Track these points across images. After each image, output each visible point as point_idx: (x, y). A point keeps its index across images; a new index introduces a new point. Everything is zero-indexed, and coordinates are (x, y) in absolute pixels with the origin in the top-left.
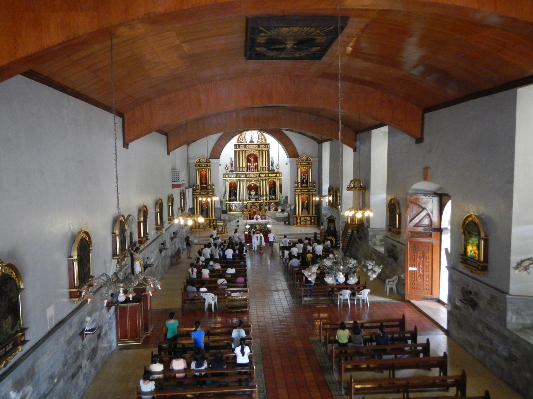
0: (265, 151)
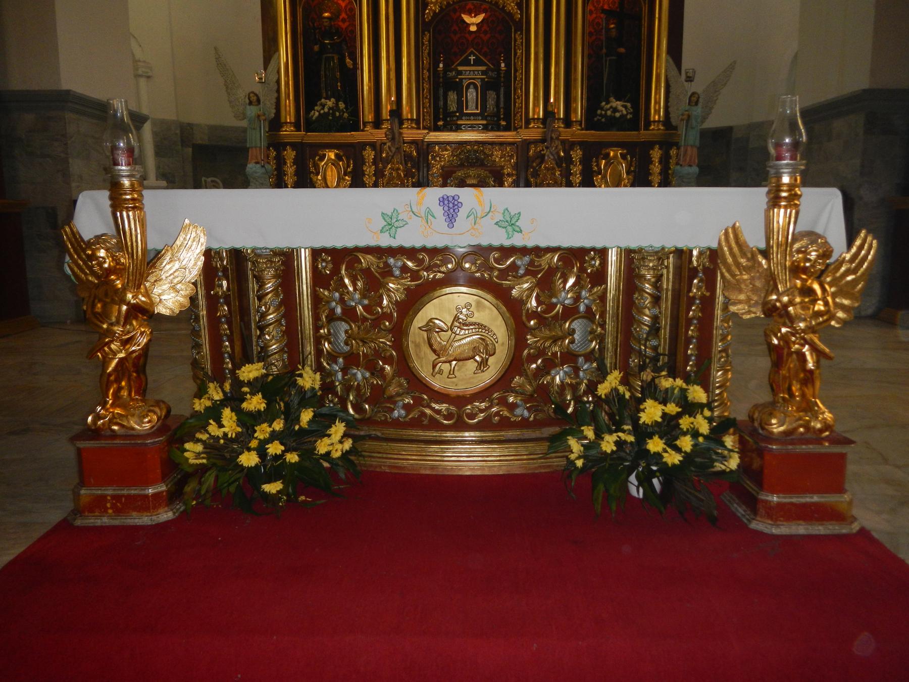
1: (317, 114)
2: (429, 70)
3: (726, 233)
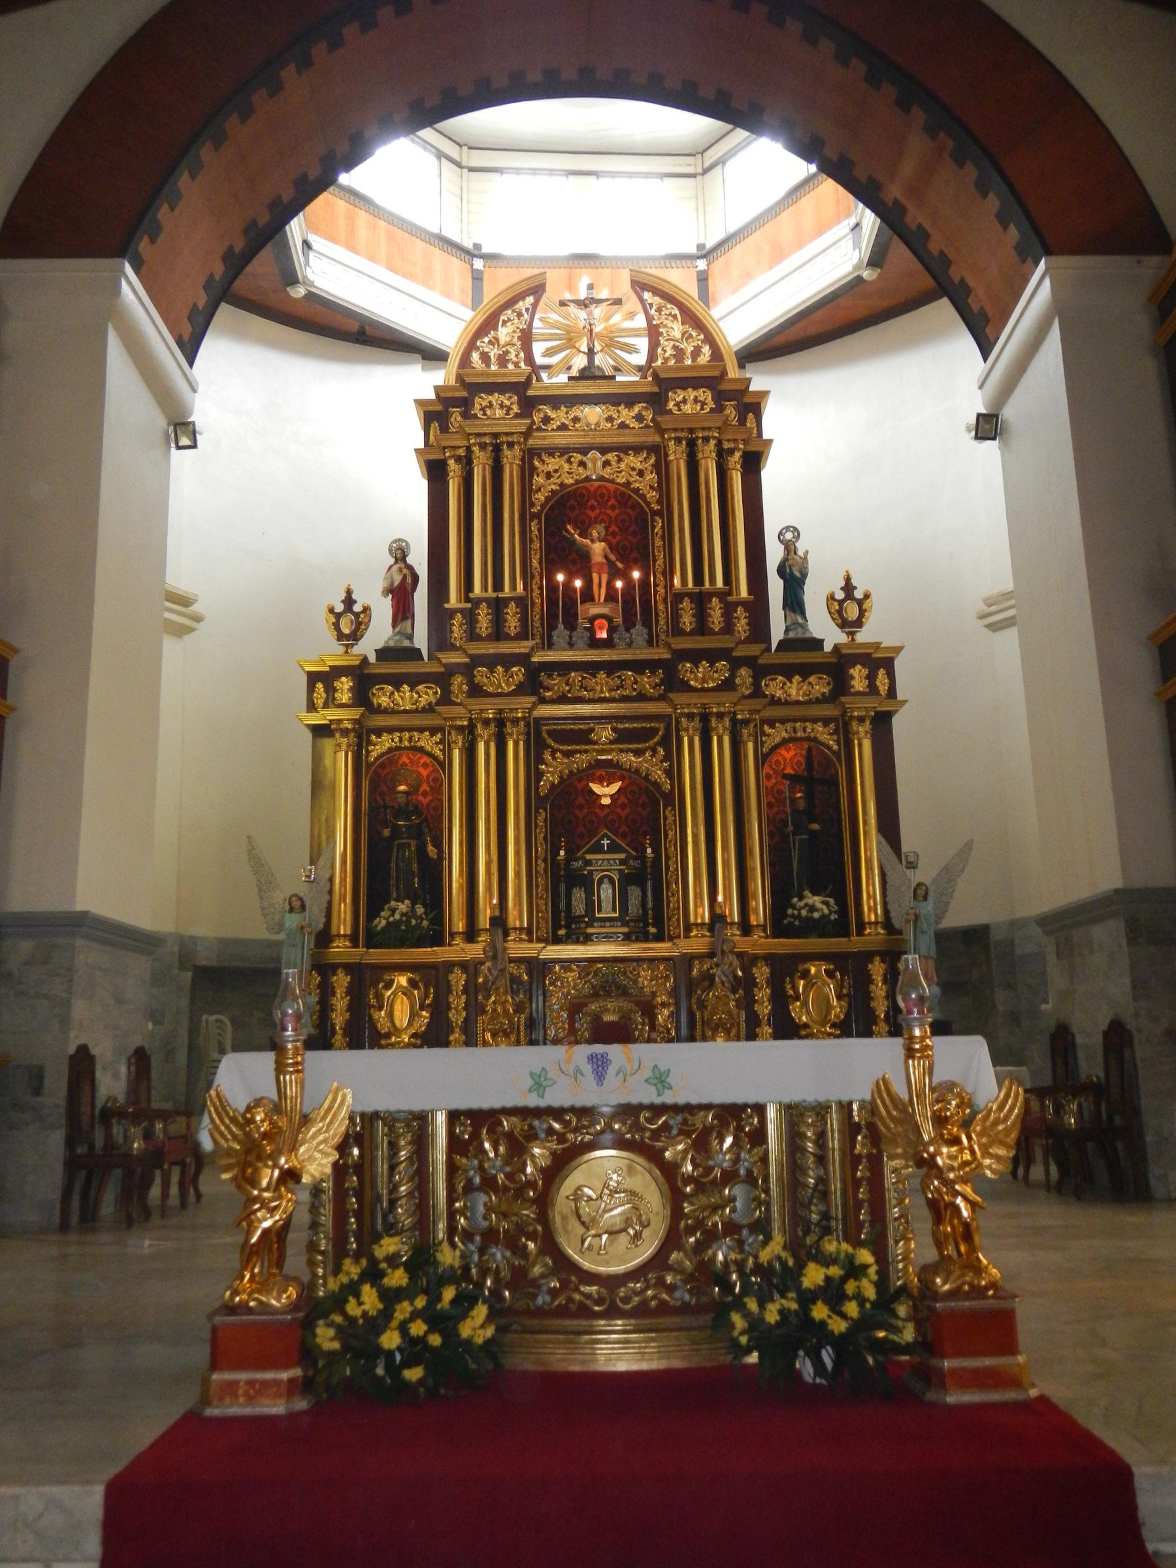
0: (722, 455)
1: (384, 922)
2: (545, 860)
3: (878, 1083)
